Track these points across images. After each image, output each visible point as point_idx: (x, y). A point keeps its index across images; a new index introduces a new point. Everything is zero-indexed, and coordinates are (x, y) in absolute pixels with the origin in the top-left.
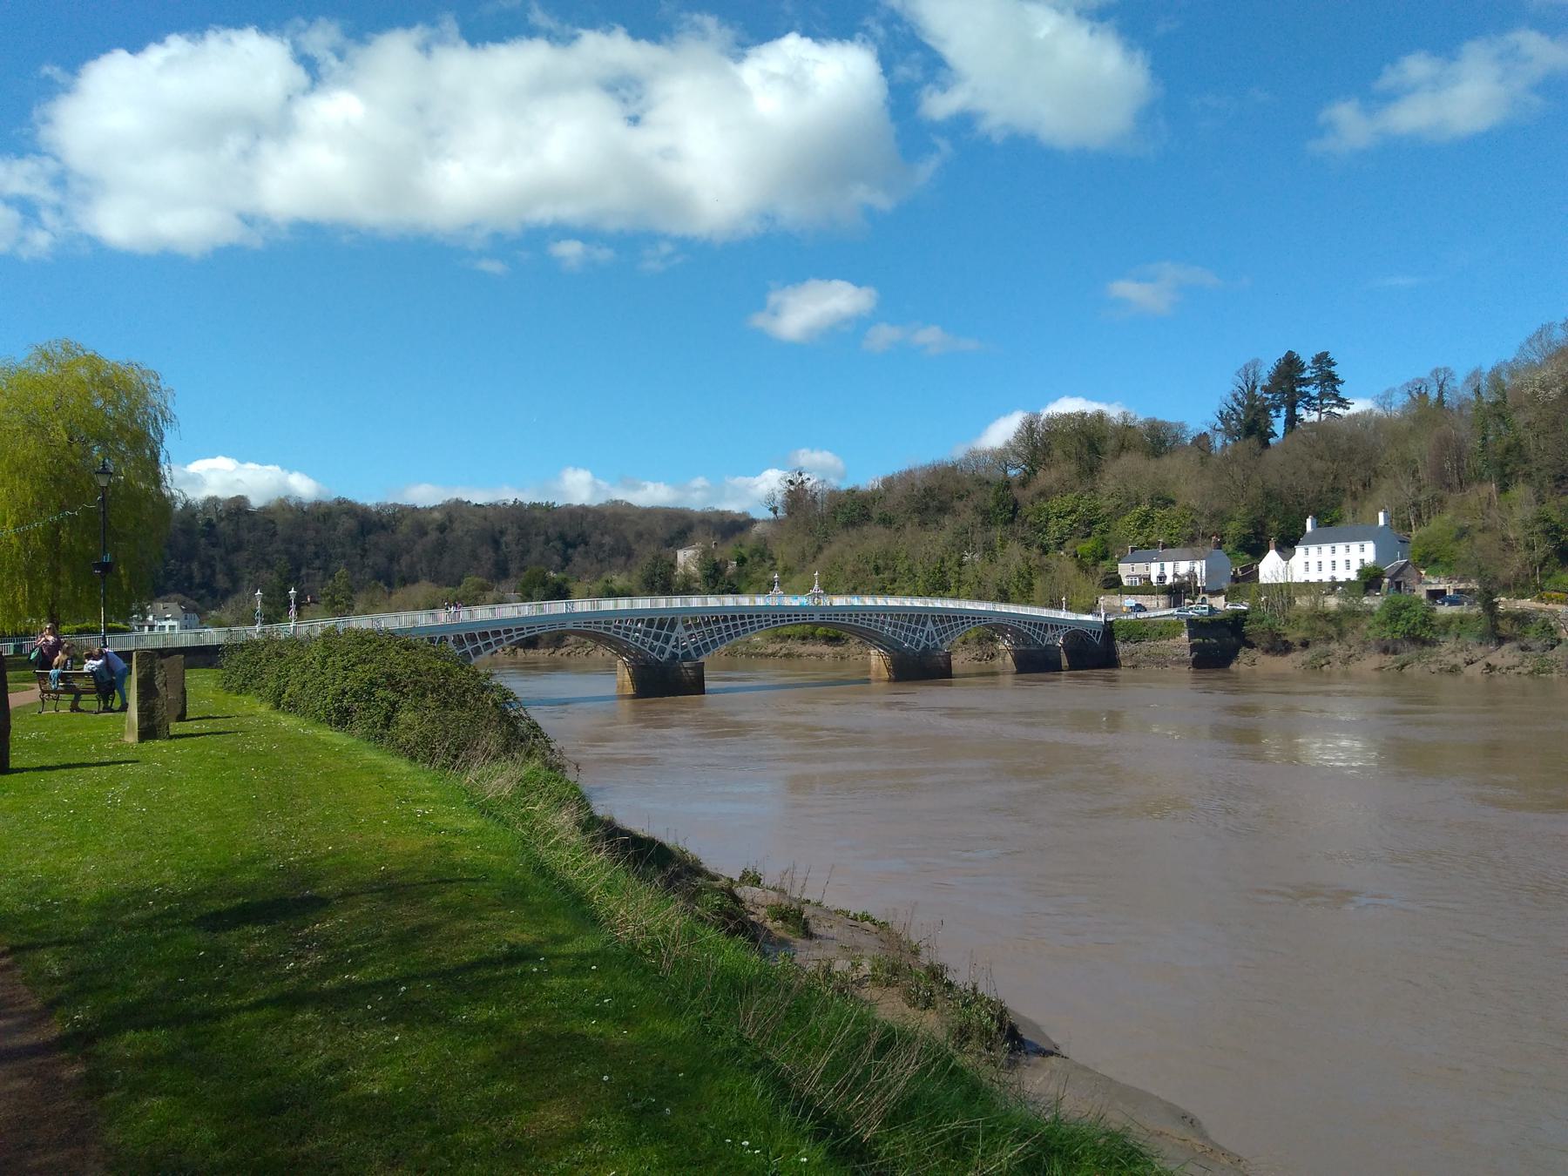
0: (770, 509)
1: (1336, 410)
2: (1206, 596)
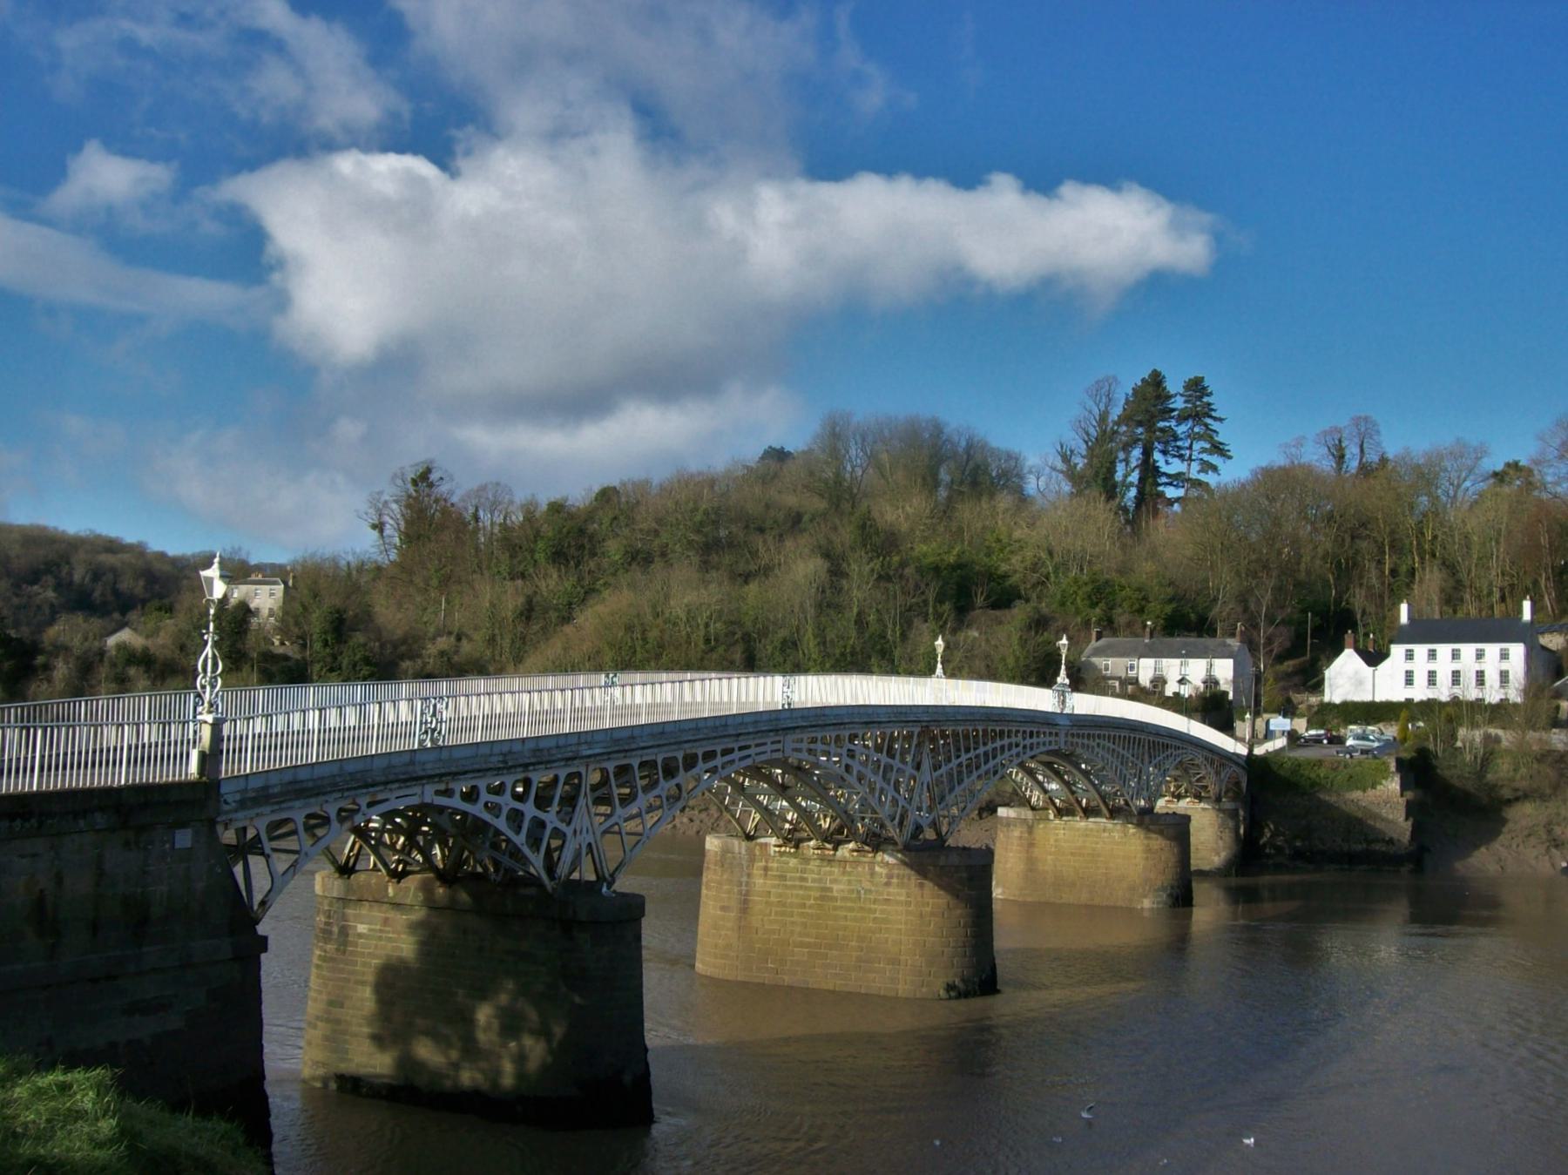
0: (374, 527)
1: (1215, 459)
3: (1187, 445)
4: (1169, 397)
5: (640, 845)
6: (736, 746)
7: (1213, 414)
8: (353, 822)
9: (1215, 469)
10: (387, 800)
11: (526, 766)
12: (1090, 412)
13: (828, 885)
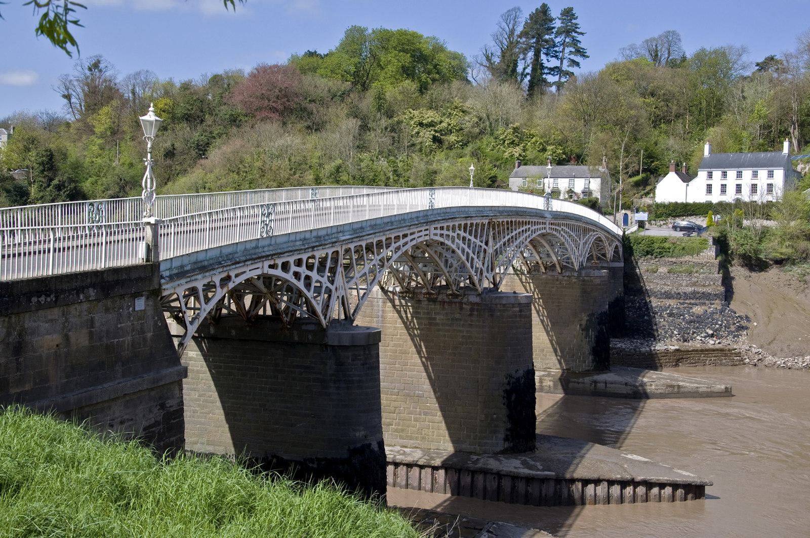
0: (65, 96)
1: (578, 59)
2: (628, 212)
3: (561, 50)
4: (551, 20)
5: (366, 295)
6: (409, 232)
7: (578, 30)
8: (228, 288)
9: (577, 64)
10: (245, 272)
11: (313, 247)
12: (504, 30)
13: (433, 316)
